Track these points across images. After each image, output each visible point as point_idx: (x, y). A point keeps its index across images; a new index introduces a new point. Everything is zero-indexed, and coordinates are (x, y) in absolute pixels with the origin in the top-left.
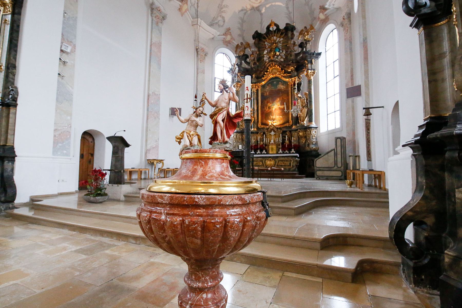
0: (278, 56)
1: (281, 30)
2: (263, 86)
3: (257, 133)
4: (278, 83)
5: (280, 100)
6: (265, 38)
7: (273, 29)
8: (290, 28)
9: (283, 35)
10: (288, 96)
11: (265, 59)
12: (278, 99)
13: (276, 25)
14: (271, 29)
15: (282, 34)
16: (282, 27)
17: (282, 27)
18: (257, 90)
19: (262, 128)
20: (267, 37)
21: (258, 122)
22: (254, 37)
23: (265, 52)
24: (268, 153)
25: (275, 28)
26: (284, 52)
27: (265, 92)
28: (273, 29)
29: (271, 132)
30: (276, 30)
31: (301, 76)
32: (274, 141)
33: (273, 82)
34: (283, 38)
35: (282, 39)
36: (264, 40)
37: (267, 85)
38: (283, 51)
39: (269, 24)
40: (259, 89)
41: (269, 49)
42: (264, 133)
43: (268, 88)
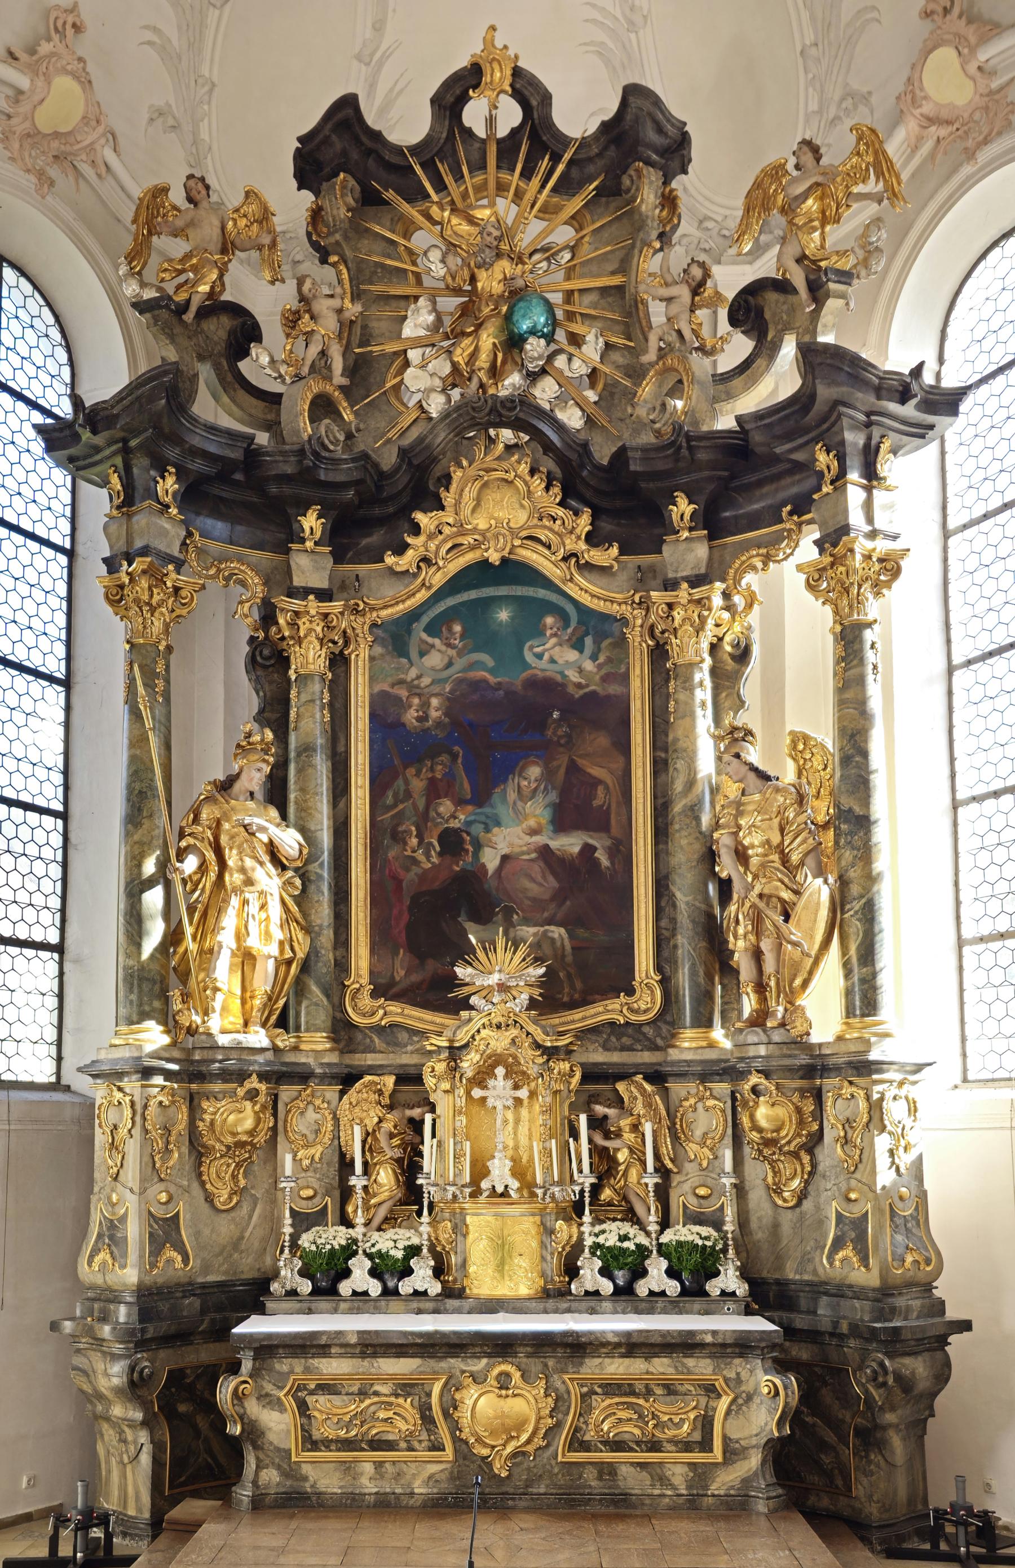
0: (533, 377)
1: (565, 141)
2: (396, 637)
3: (348, 1080)
4: (531, 615)
5: (549, 775)
6: (416, 195)
7: (491, 122)
8: (641, 141)
9: (576, 203)
10: (624, 747)
11: (415, 380)
12: (535, 771)
13: (528, 91)
14: (474, 115)
15: (566, 187)
16: (580, 112)
17: (580, 112)
18: (339, 662)
19: (379, 1030)
20: (440, 186)
21: (342, 966)
22: (311, 165)
23: (417, 322)
24: (453, 1293)
25: (510, 116)
26: (592, 348)
27: (414, 689)
28: (491, 122)
29: (481, 1078)
30: (515, 132)
31: (750, 579)
32: (520, 1171)
33: (487, 604)
34: (576, 220)
35: (564, 234)
36: (406, 207)
37: (432, 629)
38: (576, 340)
39: (462, 62)
40: (360, 657)
41: (450, 303)
42: (410, 1078)
43: (434, 660)
